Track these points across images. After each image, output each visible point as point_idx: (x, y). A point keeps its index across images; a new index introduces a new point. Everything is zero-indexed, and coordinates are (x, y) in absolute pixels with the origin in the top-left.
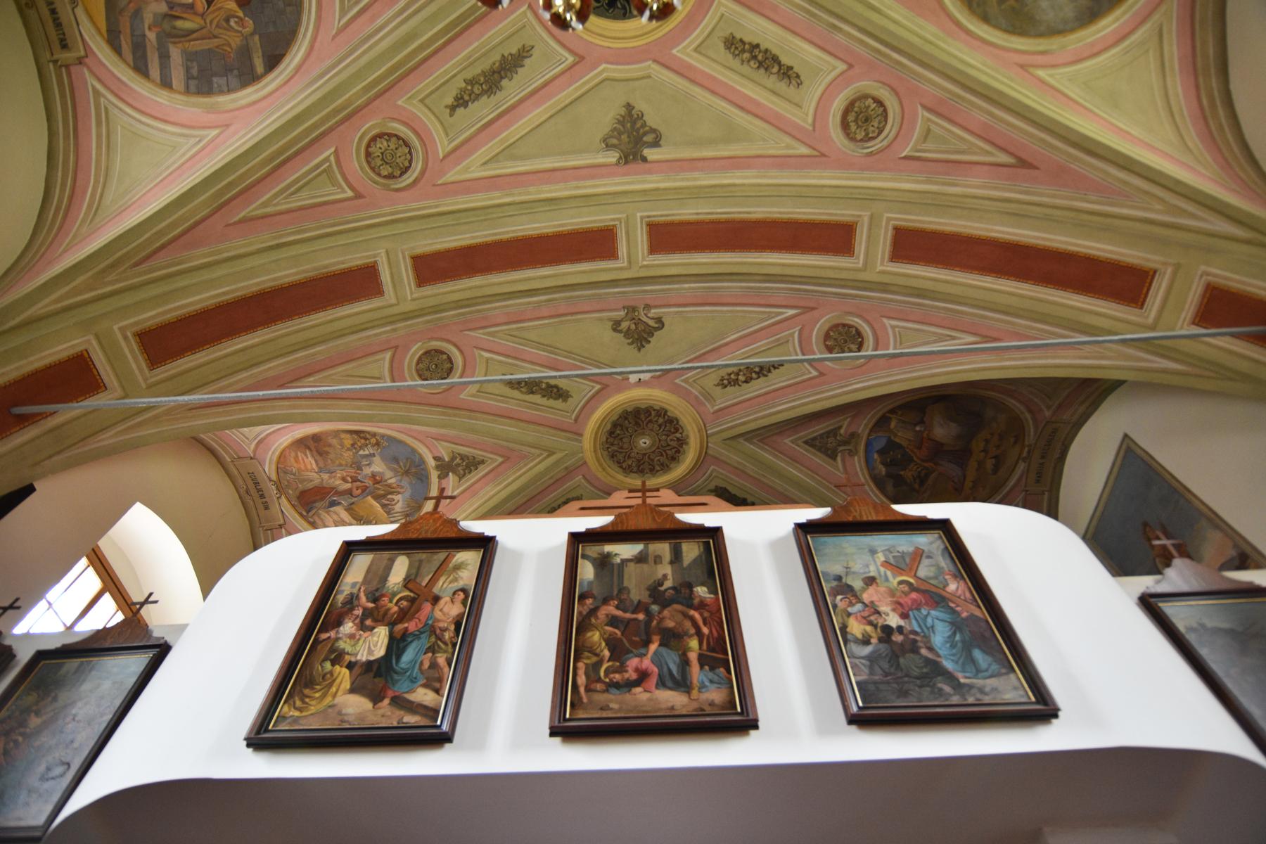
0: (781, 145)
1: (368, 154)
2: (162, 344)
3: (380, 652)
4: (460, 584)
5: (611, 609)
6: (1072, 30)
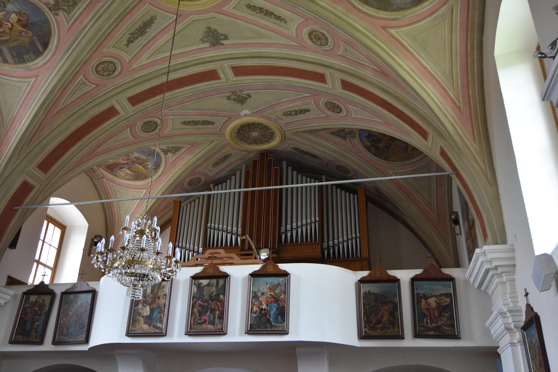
0: (285, 41)
1: (97, 72)
2: (45, 166)
3: (149, 313)
4: (164, 293)
5: (199, 302)
6: (409, 8)
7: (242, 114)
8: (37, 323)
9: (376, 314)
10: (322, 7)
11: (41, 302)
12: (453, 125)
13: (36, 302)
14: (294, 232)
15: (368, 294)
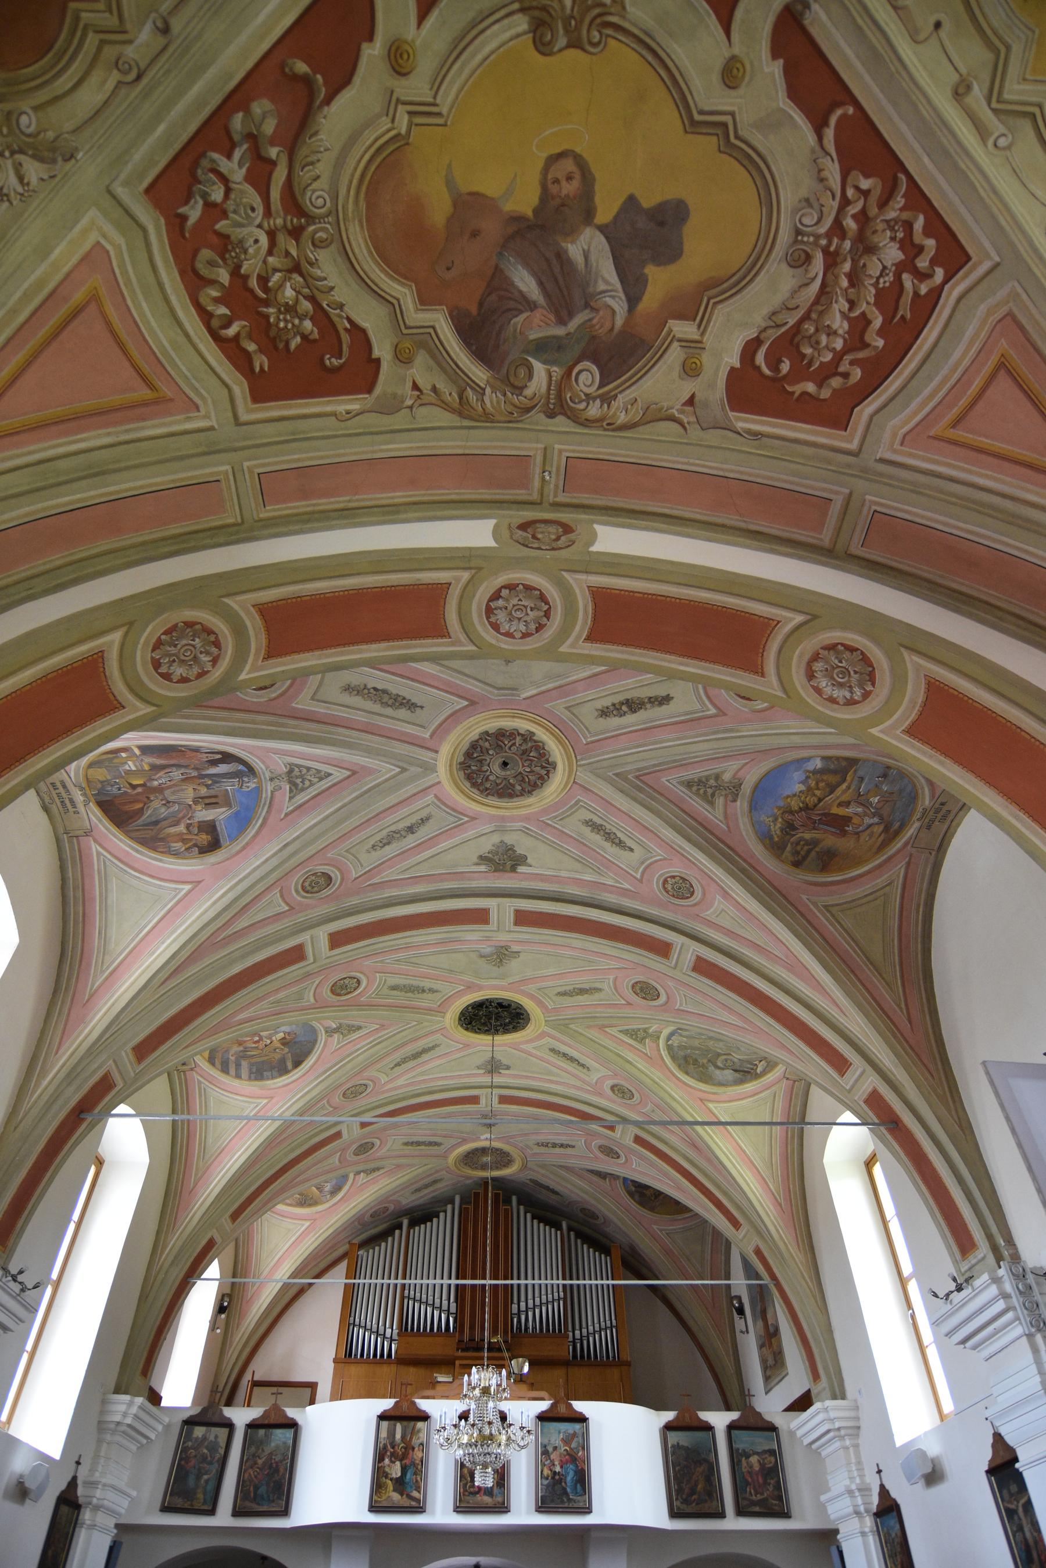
0: (579, 1084)
3: (399, 1474)
4: (420, 1441)
6: (731, 1085)
7: (482, 1137)
8: (206, 1477)
9: (689, 1481)
10: (639, 1069)
11: (212, 1438)
12: (775, 1226)
13: (204, 1438)
14: (530, 1314)
15: (677, 1447)
